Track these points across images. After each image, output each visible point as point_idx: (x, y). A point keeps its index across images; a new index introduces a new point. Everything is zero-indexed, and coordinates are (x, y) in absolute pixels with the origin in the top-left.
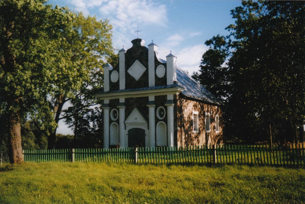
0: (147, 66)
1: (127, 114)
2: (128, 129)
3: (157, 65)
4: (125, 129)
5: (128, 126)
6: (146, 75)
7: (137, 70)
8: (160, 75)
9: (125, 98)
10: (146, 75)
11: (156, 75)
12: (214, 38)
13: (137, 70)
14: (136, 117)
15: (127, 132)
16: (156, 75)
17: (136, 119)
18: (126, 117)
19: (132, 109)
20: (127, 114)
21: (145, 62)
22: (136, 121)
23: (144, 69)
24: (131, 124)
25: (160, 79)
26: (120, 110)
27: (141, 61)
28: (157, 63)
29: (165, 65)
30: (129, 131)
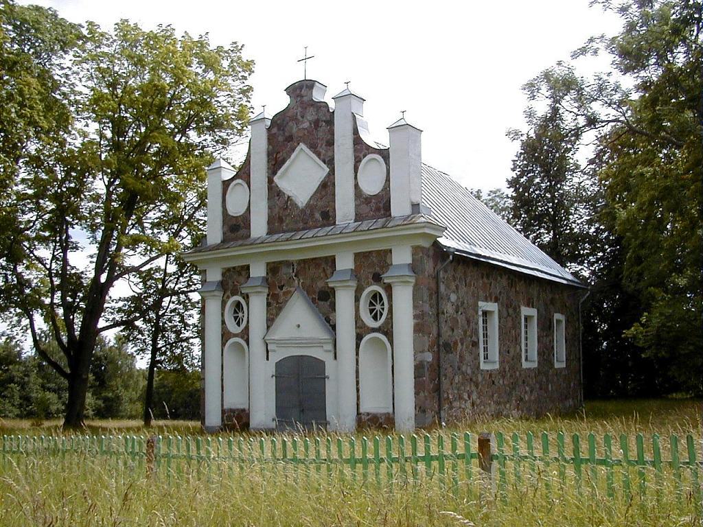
0: (330, 162)
1: (275, 308)
2: (275, 357)
3: (361, 155)
4: (268, 359)
5: (274, 351)
6: (327, 187)
7: (301, 177)
8: (371, 186)
9: (268, 264)
10: (327, 187)
11: (356, 186)
12: (547, 76)
13: (301, 177)
14: (299, 319)
15: (272, 370)
16: (356, 186)
17: (299, 326)
18: (270, 322)
19: (289, 294)
20: (275, 308)
21: (323, 146)
22: (296, 334)
23: (321, 172)
24: (282, 343)
25: (368, 200)
26: (250, 298)
27: (313, 147)
28: (361, 148)
29: (385, 154)
30: (279, 365)
